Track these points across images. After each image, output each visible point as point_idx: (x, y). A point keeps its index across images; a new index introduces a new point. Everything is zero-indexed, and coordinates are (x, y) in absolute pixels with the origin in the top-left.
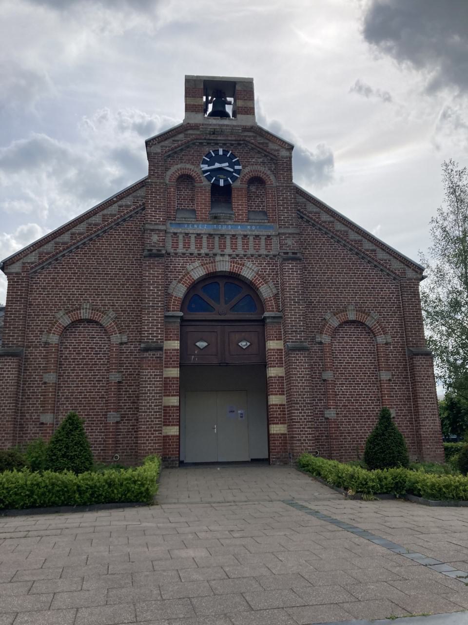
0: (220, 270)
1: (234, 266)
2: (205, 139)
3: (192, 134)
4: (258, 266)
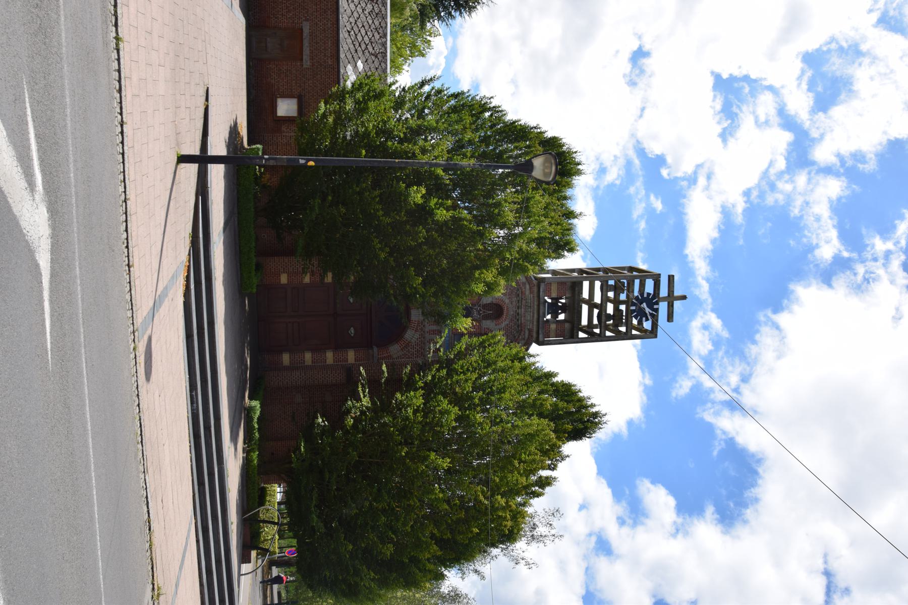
0: (412, 312)
1: (415, 323)
2: (522, 299)
3: (525, 288)
4: (415, 342)
